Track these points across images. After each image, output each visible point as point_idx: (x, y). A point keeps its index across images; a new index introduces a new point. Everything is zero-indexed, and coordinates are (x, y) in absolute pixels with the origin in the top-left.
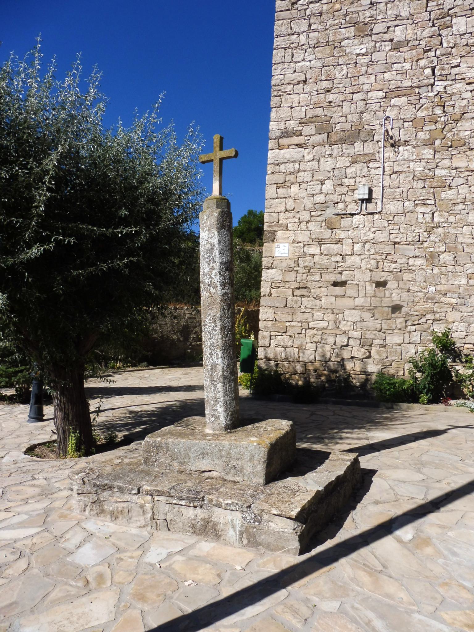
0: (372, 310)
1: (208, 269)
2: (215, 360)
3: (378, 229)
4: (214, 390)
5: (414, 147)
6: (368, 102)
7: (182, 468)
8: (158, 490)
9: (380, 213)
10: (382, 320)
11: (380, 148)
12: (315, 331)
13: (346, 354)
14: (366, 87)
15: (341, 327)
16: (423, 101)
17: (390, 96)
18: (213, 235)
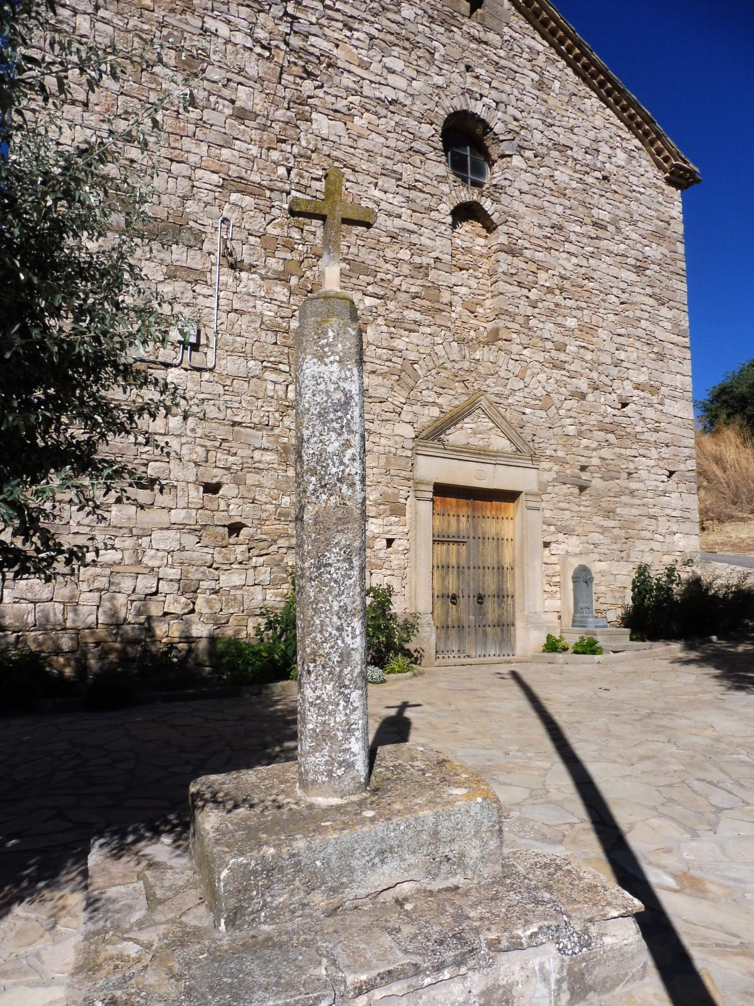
0: (198, 531)
1: (336, 444)
2: (348, 640)
3: (209, 397)
4: (345, 708)
5: (263, 279)
6: (195, 183)
7: (335, 901)
8: (390, 972)
9: (211, 370)
10: (214, 548)
11: (213, 264)
12: (98, 570)
13: (155, 610)
14: (193, 159)
15: (145, 560)
16: (275, 212)
17: (230, 187)
18: (348, 373)
